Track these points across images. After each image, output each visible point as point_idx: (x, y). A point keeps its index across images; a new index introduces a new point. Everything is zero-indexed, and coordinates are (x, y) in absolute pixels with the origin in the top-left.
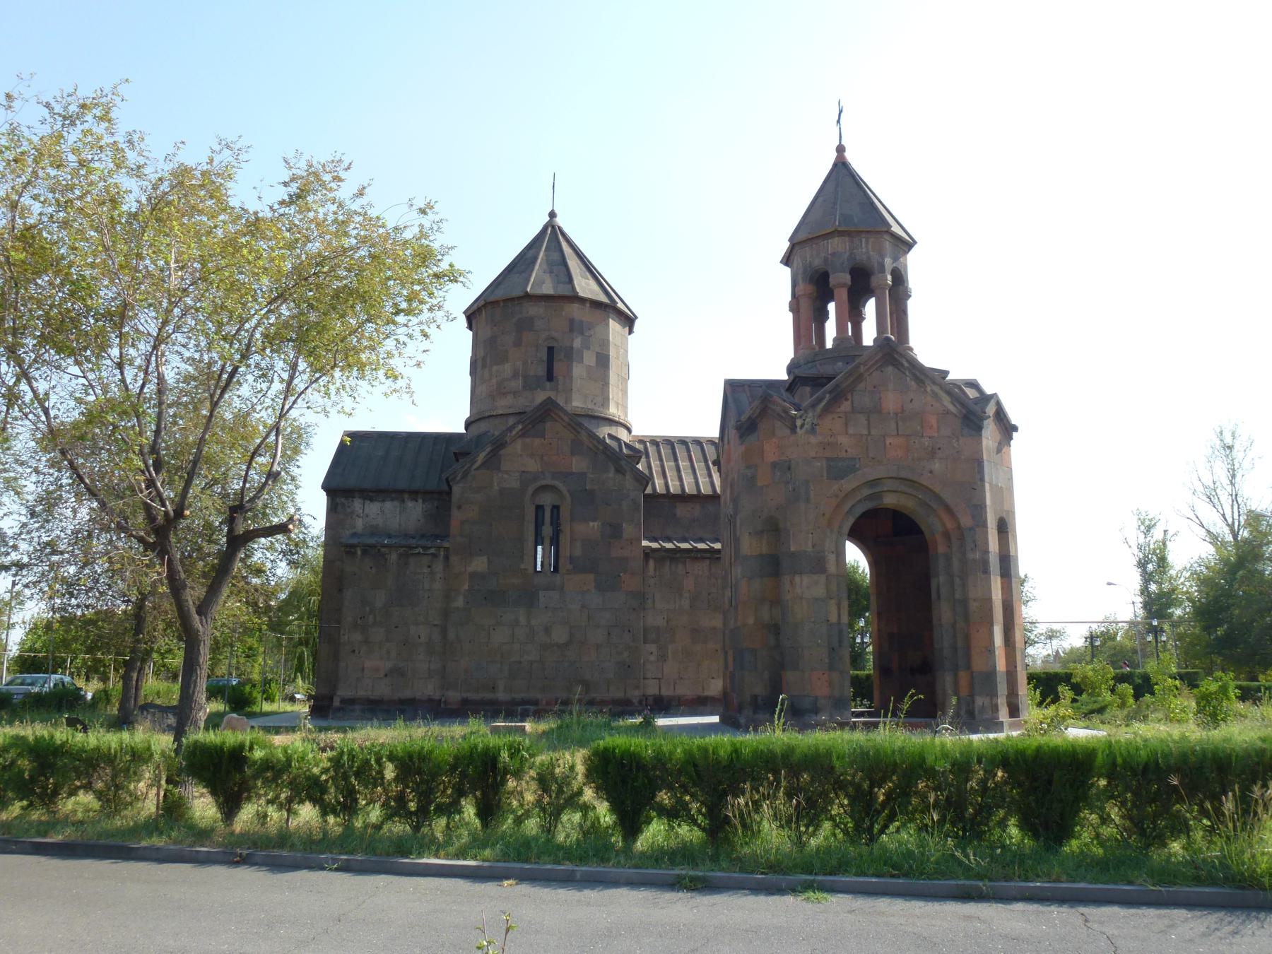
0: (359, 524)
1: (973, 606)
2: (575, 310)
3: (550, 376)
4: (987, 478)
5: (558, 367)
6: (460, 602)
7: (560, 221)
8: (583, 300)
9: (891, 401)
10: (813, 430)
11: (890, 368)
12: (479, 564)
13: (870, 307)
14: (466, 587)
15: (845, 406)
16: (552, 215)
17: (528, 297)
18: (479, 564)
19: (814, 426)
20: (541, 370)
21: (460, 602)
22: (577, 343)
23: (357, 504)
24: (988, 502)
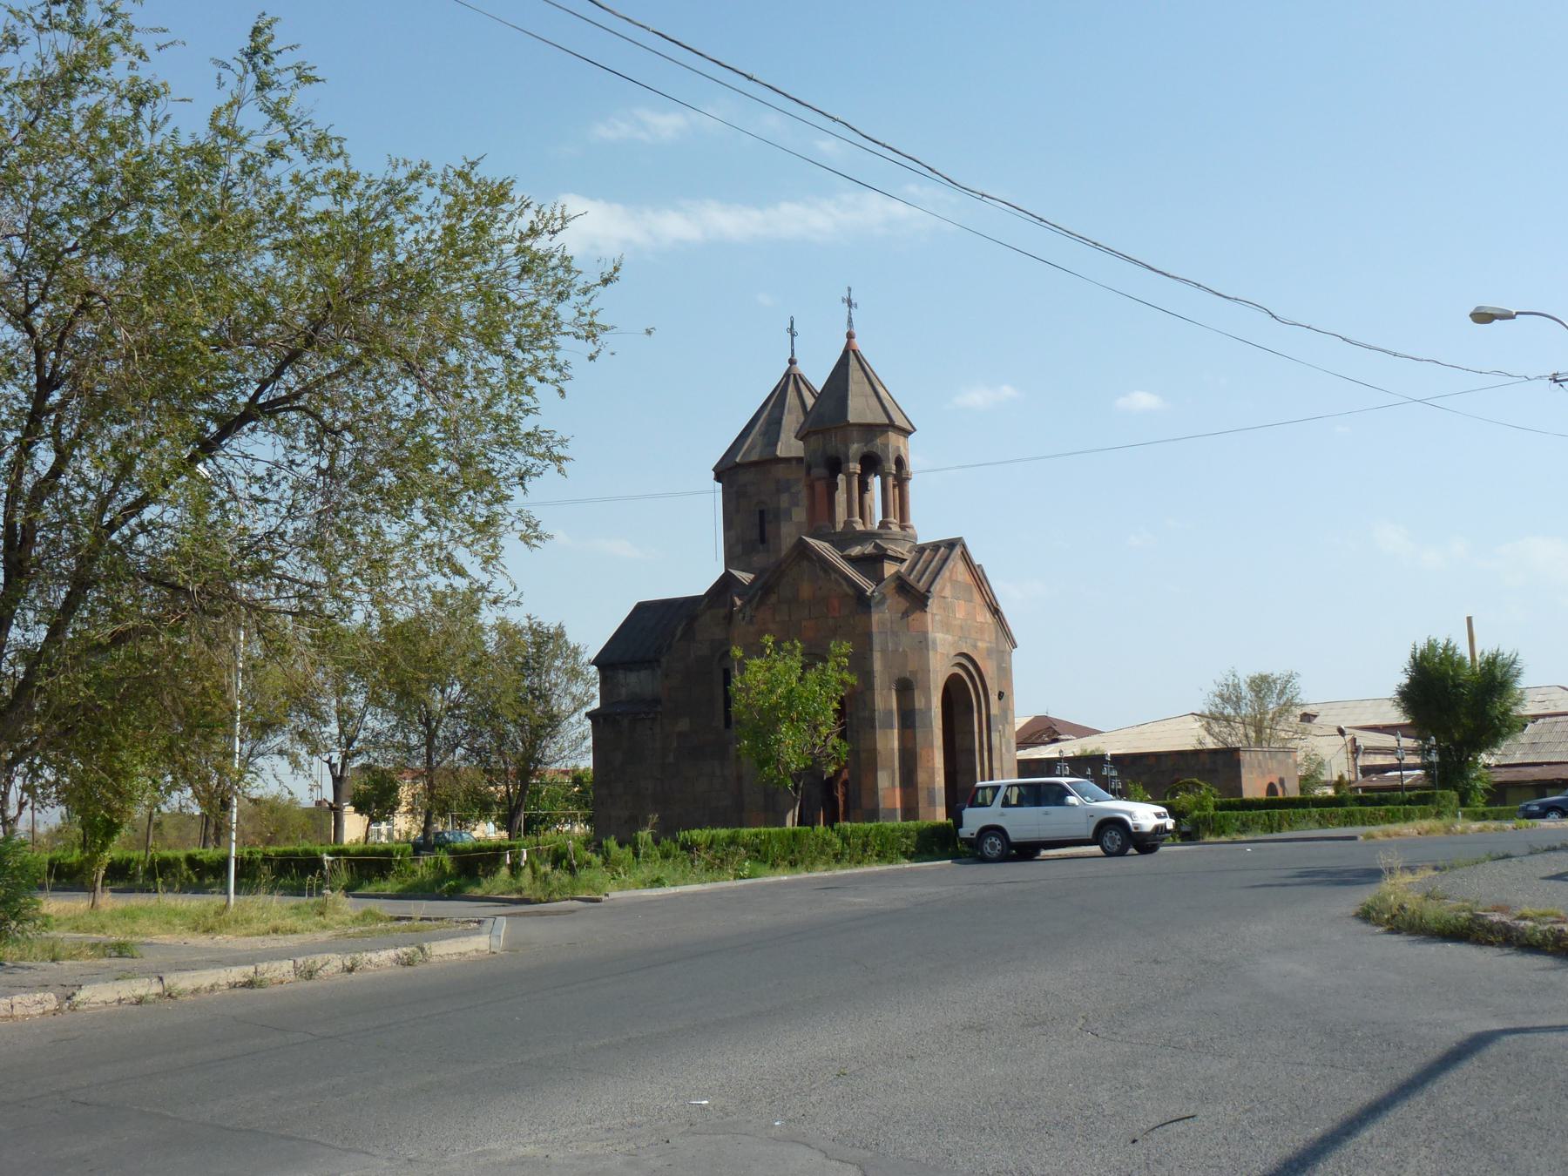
0: (623, 691)
1: (863, 755)
2: (780, 471)
3: (763, 540)
4: (877, 647)
5: (768, 527)
6: (671, 759)
7: (801, 368)
8: (787, 460)
9: (806, 591)
10: (751, 622)
11: (805, 563)
12: (683, 725)
13: (875, 483)
14: (675, 744)
15: (773, 599)
16: (792, 362)
17: (738, 465)
18: (683, 725)
19: (752, 617)
20: (755, 534)
21: (671, 759)
22: (784, 500)
23: (621, 675)
24: (877, 666)
